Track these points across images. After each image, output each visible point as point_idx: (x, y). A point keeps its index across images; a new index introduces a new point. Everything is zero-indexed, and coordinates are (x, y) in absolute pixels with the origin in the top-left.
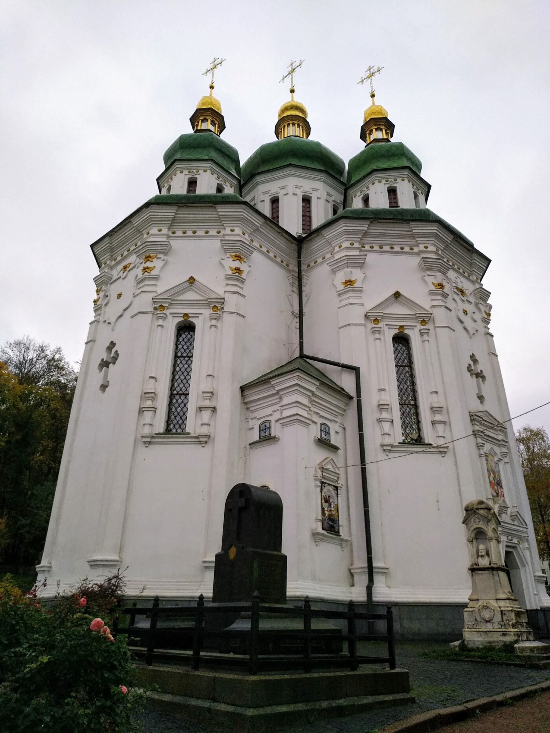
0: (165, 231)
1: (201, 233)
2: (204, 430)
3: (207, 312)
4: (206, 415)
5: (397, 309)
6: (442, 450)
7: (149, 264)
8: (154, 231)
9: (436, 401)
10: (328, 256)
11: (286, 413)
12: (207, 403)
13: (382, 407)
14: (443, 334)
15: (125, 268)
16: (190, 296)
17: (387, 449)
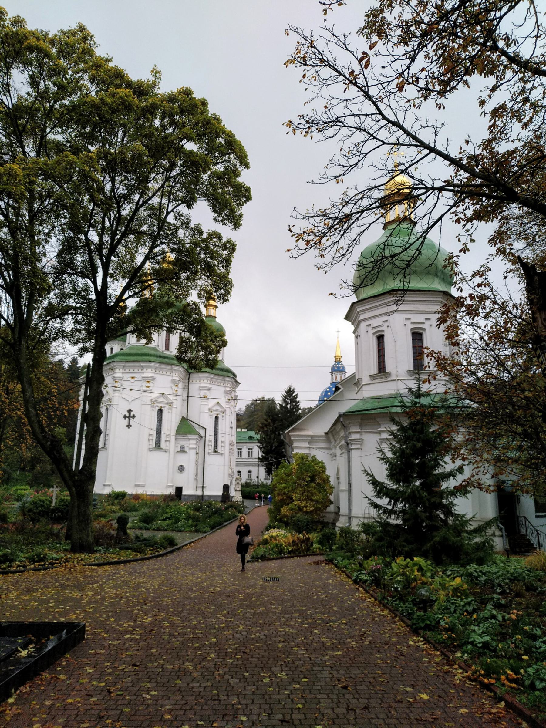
0: (154, 371)
1: (164, 373)
2: (167, 448)
3: (167, 406)
4: (168, 443)
5: (217, 408)
6: (222, 455)
7: (148, 385)
8: (149, 370)
9: (223, 440)
10: (198, 381)
11: (191, 446)
12: (168, 439)
13: (210, 441)
14: (227, 417)
15: (133, 378)
16: (162, 399)
17: (209, 454)
